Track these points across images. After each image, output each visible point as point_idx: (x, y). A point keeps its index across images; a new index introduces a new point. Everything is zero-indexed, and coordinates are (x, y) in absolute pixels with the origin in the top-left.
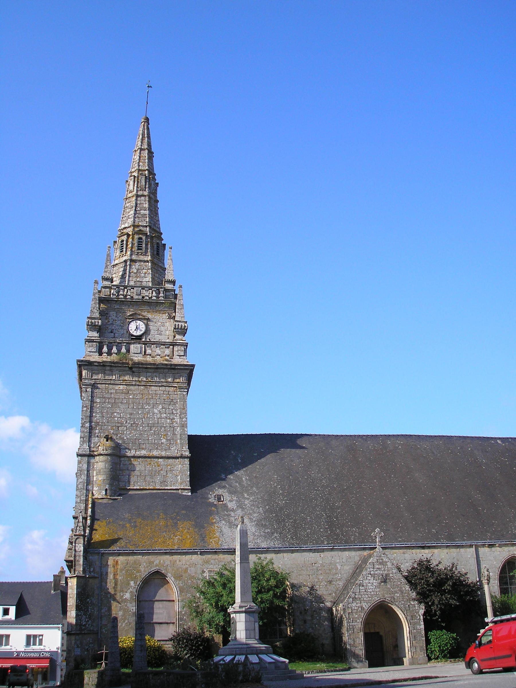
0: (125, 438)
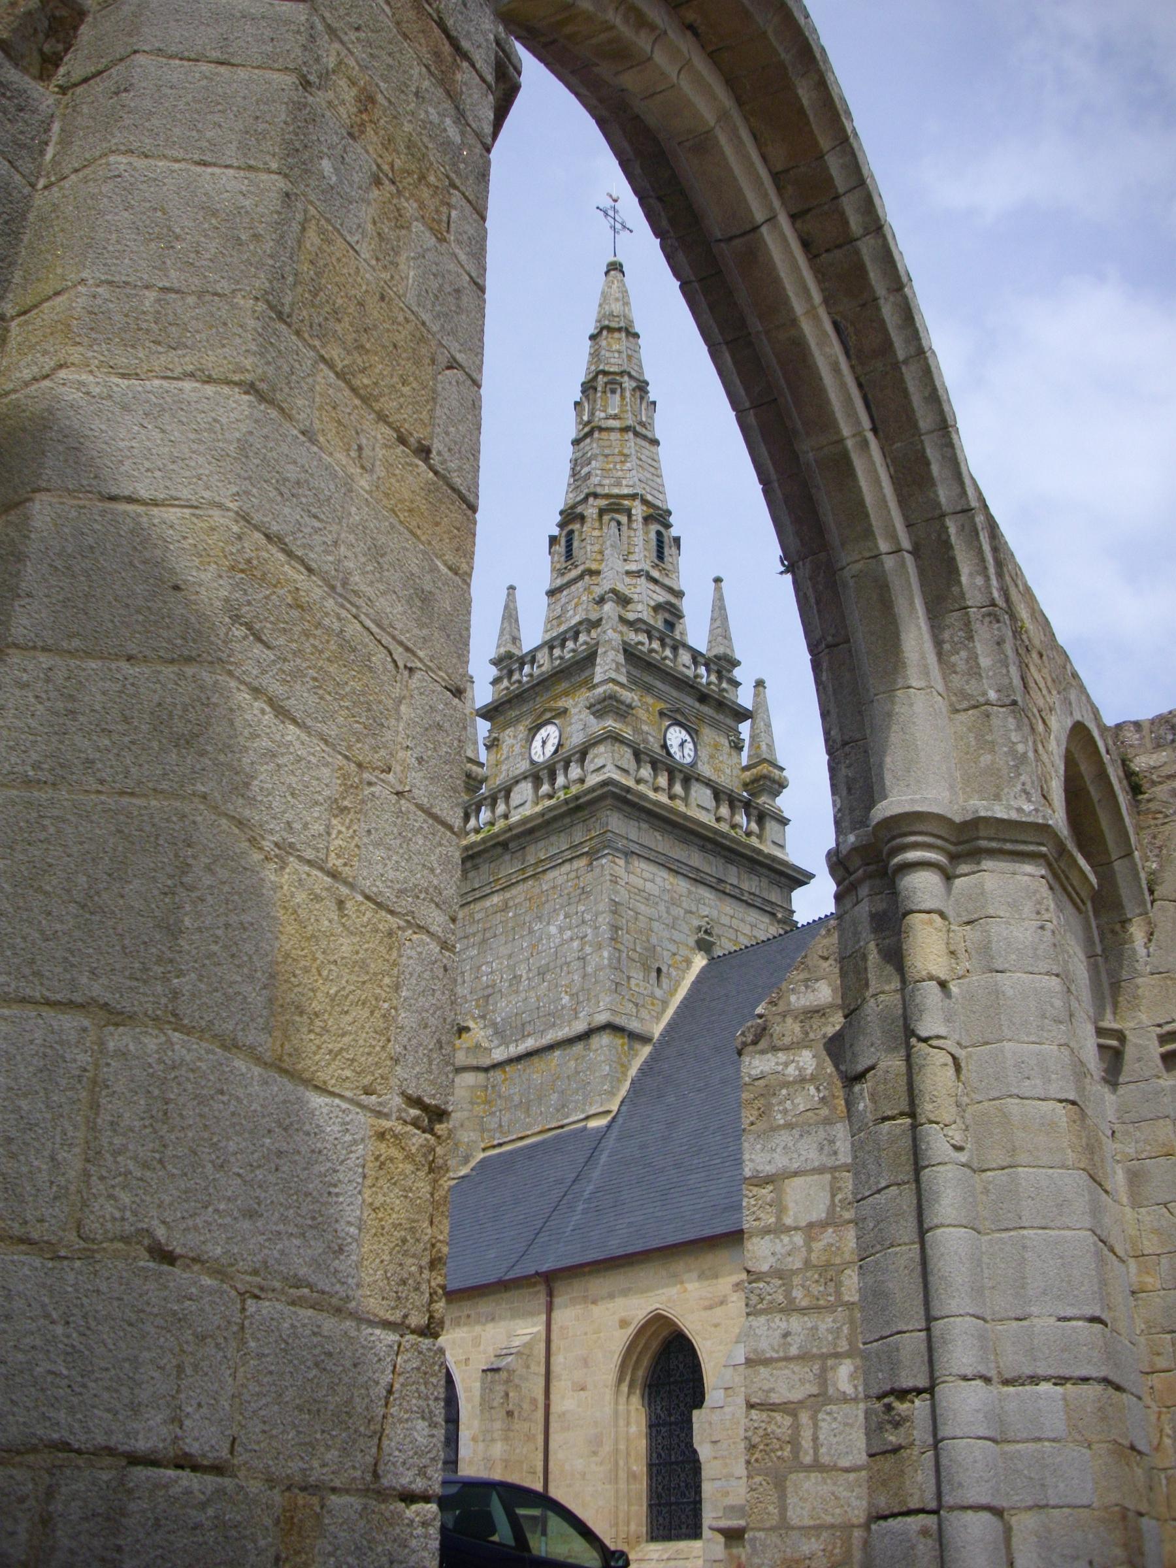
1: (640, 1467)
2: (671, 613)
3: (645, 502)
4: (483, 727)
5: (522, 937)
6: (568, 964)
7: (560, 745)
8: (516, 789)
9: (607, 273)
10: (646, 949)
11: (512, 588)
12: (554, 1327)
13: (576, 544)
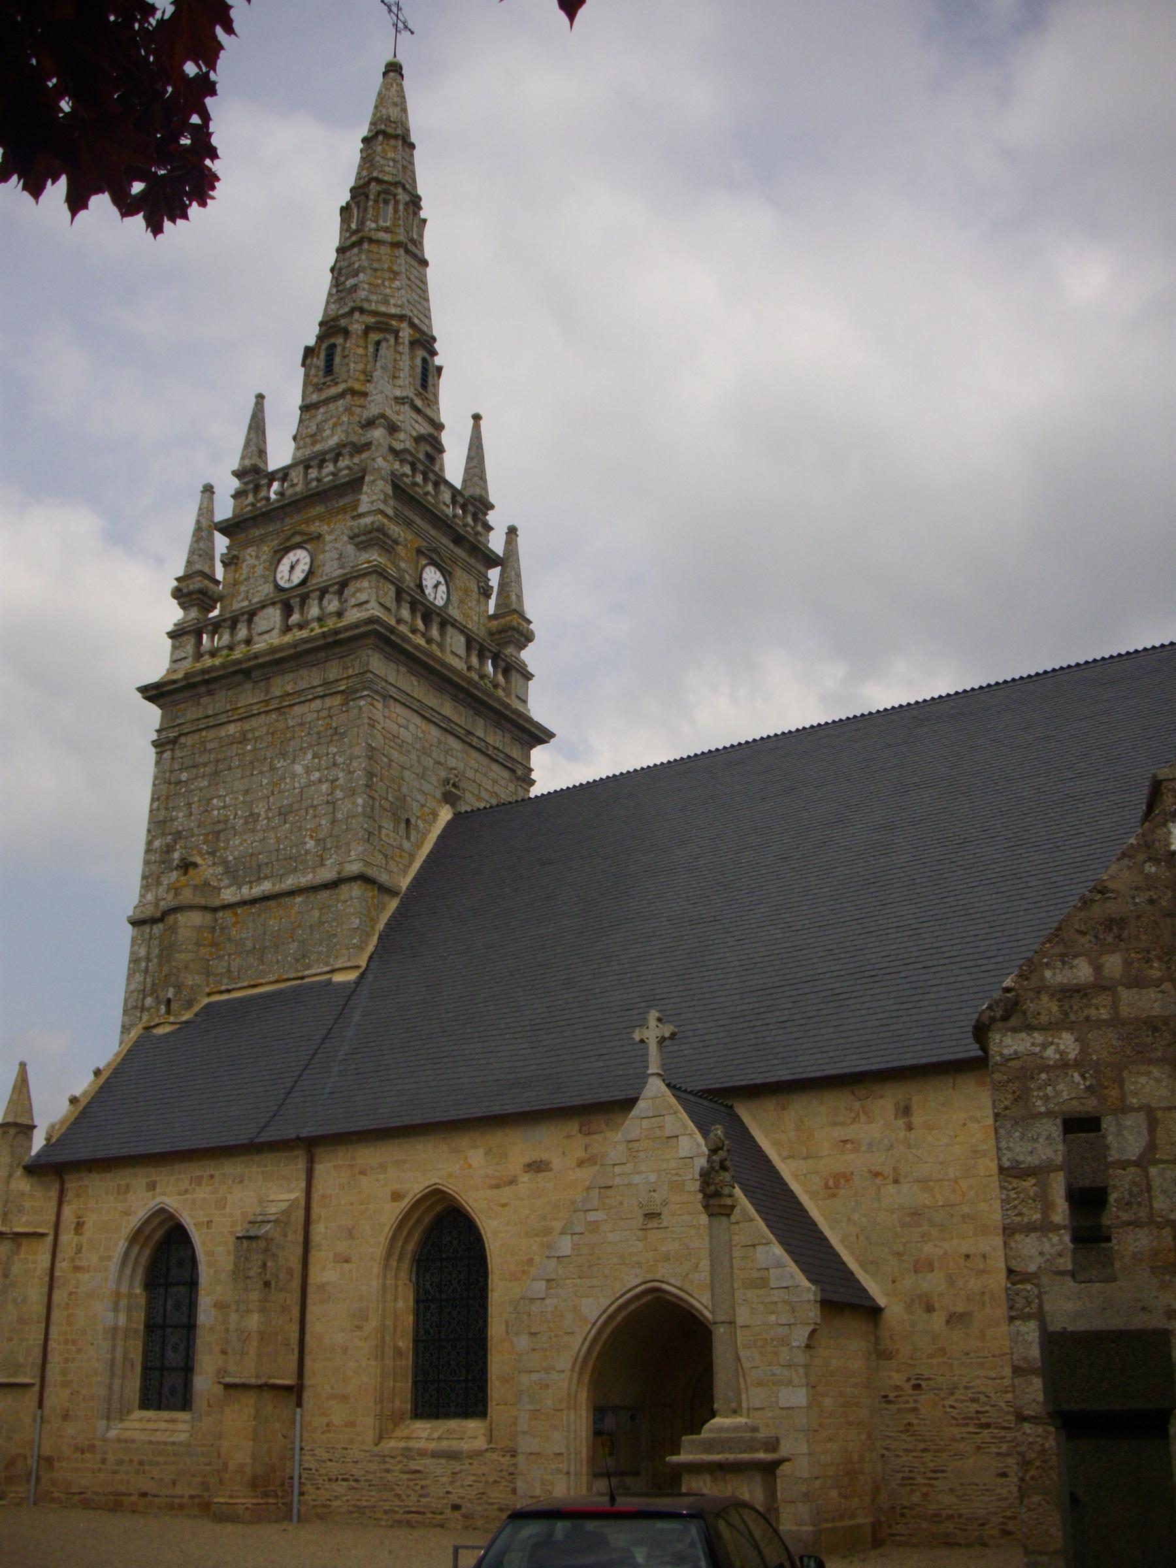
0: (231, 858)
1: (405, 1343)
2: (433, 446)
3: (412, 325)
4: (221, 543)
5: (262, 773)
6: (315, 807)
7: (311, 573)
8: (263, 614)
9: (385, 74)
10: (398, 799)
11: (260, 397)
12: (315, 1195)
13: (337, 360)
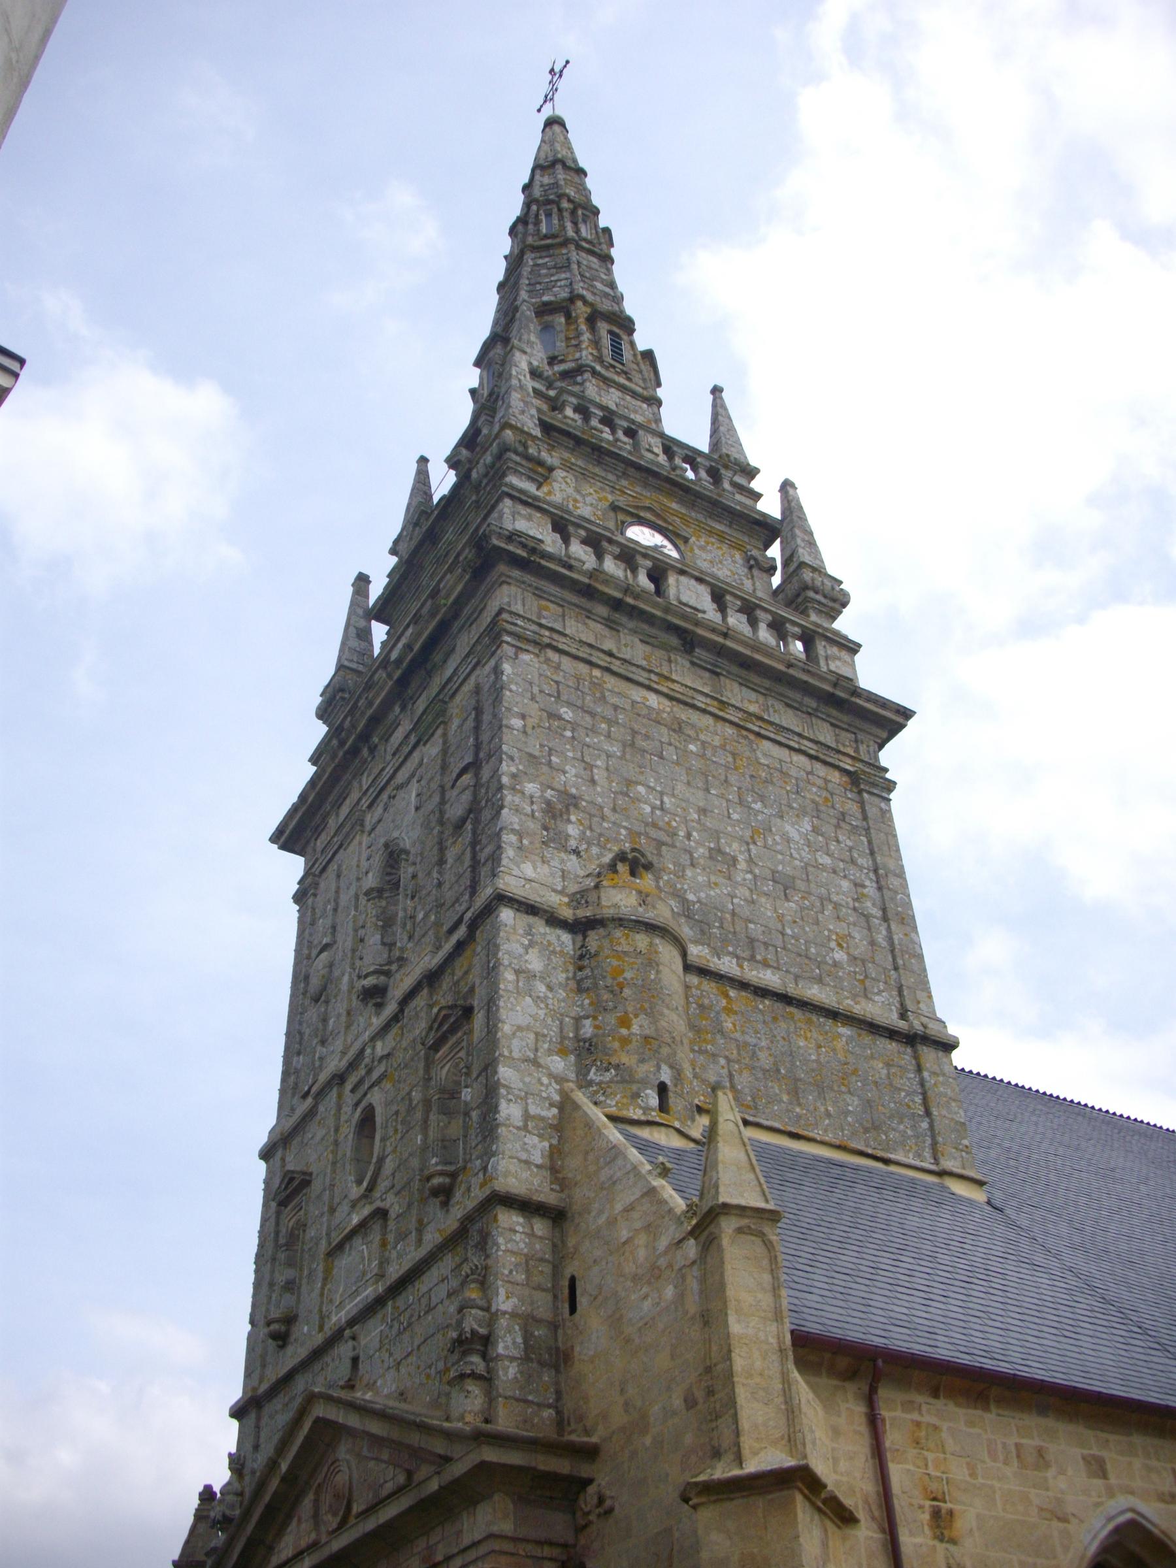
0: (691, 897)
6: (837, 906)
